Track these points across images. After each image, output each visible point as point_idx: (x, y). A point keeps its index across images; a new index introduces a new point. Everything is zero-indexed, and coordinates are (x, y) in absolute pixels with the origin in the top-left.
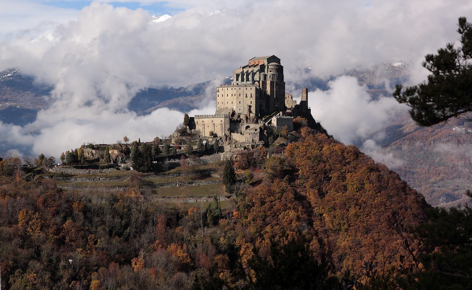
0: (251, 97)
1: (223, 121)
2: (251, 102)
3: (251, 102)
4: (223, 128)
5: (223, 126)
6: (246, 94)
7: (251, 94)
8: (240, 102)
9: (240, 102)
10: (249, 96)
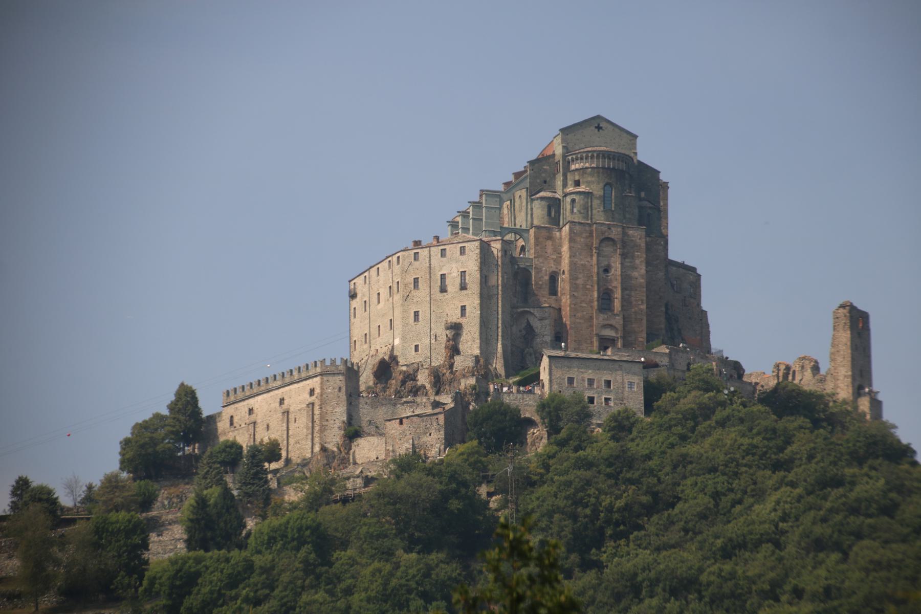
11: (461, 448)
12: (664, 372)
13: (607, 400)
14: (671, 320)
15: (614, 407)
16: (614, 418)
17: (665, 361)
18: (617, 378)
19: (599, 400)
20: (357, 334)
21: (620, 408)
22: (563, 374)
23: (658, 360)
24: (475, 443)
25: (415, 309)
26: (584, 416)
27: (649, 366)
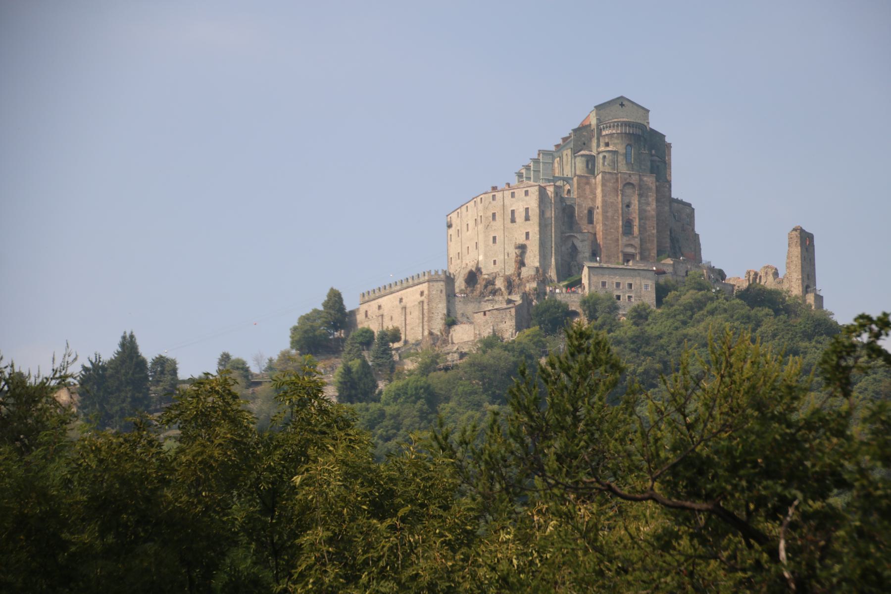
0: (527, 219)
1: (426, 292)
2: (527, 234)
3: (527, 234)
4: (426, 311)
5: (426, 307)
6: (513, 212)
7: (527, 209)
8: (494, 238)
9: (494, 238)
11: (527, 332)
12: (669, 277)
13: (630, 297)
14: (674, 240)
15: (635, 302)
16: (635, 310)
17: (670, 270)
18: (636, 281)
19: (624, 298)
20: (453, 253)
22: (598, 280)
23: (665, 269)
24: (537, 328)
25: (496, 236)
27: (660, 273)
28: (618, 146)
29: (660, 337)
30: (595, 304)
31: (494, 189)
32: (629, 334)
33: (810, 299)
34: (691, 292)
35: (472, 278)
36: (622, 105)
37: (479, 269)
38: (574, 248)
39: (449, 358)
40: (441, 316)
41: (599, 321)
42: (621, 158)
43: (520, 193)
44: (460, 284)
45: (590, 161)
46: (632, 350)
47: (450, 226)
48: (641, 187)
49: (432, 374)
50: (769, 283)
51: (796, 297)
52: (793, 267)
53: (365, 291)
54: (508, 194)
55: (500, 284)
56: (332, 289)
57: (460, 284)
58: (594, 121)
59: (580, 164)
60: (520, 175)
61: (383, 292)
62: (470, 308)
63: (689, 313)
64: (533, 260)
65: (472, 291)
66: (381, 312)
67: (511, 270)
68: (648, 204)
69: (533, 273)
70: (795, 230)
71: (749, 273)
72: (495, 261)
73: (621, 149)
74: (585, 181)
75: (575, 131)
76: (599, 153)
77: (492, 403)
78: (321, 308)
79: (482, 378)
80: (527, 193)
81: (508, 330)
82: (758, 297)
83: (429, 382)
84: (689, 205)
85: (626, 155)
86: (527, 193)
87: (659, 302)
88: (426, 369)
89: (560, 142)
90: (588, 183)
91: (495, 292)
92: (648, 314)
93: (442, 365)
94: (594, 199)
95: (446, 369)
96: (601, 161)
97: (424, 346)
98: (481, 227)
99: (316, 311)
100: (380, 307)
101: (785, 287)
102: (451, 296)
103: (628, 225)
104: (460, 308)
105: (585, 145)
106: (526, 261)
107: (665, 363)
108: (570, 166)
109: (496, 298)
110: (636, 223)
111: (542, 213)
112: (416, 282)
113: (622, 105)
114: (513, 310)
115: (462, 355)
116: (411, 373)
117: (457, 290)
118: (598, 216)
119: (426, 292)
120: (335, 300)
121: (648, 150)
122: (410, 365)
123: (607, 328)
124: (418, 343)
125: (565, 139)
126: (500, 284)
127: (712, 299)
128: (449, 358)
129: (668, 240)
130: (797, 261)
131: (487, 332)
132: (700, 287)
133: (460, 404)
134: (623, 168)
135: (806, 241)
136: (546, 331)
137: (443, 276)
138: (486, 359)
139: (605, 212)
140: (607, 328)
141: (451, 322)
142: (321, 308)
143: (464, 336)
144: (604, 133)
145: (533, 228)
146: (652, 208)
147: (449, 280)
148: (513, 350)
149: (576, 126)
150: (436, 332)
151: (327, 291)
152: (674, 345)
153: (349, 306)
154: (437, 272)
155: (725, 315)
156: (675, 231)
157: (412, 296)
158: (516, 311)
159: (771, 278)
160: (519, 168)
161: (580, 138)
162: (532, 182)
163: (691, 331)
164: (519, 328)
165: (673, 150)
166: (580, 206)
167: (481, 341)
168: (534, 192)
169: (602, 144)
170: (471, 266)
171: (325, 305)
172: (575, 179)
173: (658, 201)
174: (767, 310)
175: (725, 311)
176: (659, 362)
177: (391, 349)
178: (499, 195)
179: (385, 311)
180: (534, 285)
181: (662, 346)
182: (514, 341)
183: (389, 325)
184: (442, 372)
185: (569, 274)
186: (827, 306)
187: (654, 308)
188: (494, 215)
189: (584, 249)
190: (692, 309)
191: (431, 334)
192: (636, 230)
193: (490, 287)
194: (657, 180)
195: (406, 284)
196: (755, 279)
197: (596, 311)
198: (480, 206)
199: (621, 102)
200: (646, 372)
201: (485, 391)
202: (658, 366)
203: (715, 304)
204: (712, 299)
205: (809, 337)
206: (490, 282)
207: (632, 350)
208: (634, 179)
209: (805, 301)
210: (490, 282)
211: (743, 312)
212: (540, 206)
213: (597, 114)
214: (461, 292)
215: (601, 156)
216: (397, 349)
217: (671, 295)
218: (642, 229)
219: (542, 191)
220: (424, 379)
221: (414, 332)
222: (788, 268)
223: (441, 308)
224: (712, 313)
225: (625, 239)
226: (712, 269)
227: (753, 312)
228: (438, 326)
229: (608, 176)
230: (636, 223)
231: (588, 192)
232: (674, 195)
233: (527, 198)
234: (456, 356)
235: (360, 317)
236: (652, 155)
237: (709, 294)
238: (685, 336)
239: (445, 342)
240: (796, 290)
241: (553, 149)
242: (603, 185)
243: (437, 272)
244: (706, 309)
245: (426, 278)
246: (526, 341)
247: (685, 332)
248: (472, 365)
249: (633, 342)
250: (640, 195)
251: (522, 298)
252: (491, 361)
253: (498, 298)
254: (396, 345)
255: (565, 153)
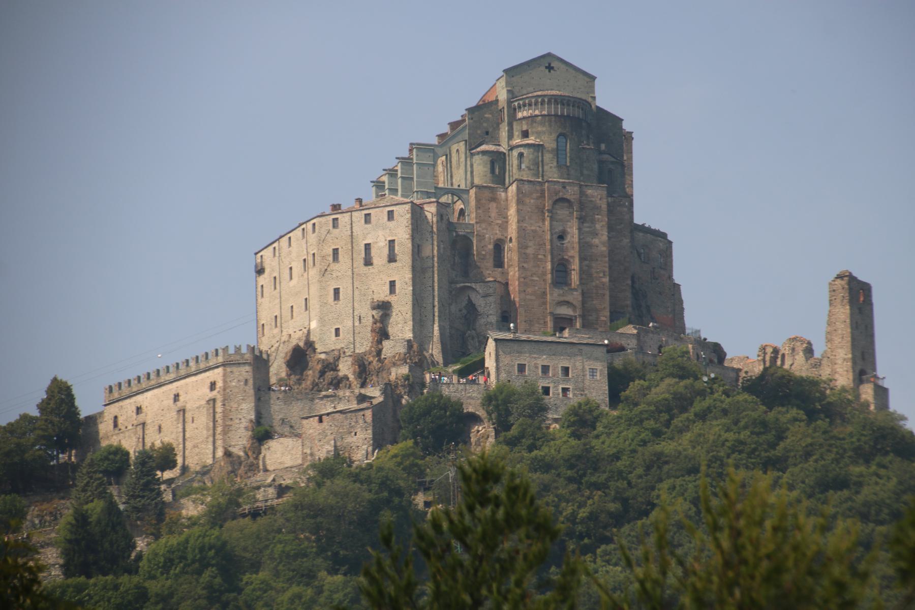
0: (392, 258)
1: (220, 384)
2: (392, 284)
3: (392, 284)
4: (219, 416)
5: (219, 409)
6: (368, 247)
7: (392, 242)
8: (337, 291)
9: (337, 291)
10: (380, 255)
11: (394, 449)
13: (565, 390)
14: (638, 295)
15: (574, 399)
16: (574, 412)
17: (632, 344)
18: (577, 364)
19: (556, 391)
20: (265, 317)
21: (581, 399)
22: (511, 361)
23: (623, 342)
24: (410, 443)
26: (539, 409)
27: (613, 349)
28: (544, 136)
29: (617, 457)
30: (506, 401)
31: (336, 208)
32: (565, 451)
33: (867, 393)
34: (668, 381)
35: (299, 358)
36: (550, 68)
37: (310, 344)
38: (471, 307)
39: (260, 495)
40: (245, 423)
41: (514, 431)
42: (548, 157)
43: (380, 215)
44: (278, 369)
45: (497, 161)
46: (570, 480)
47: (260, 271)
48: (582, 206)
49: (229, 524)
50: (797, 365)
51: (844, 389)
52: (837, 340)
53: (113, 382)
54: (359, 216)
55: (346, 368)
56: (55, 380)
57: (278, 369)
58: (502, 95)
59: (480, 167)
60: (379, 185)
61: (144, 384)
62: (296, 410)
63: (665, 417)
64: (402, 328)
65: (299, 382)
66: (141, 417)
67: (364, 345)
68: (595, 234)
69: (402, 349)
70: (840, 277)
71: (763, 349)
72: (338, 330)
73: (549, 141)
74: (488, 194)
75: (470, 110)
76: (512, 149)
77: (333, 571)
78: (35, 413)
79: (316, 530)
80: (391, 215)
81: (360, 446)
82: (779, 388)
83: (225, 536)
84: (664, 236)
85: (557, 152)
86: (391, 215)
87: (615, 398)
88: (219, 515)
89: (446, 129)
90: (494, 199)
91: (337, 383)
92: (597, 419)
93: (246, 508)
94: (504, 226)
95: (255, 514)
96: (516, 162)
97: (216, 475)
98: (313, 272)
99: (25, 418)
100: (139, 410)
101: (825, 373)
102: (262, 389)
103: (561, 270)
104: (277, 409)
105: (489, 135)
106: (391, 330)
107: (625, 501)
108: (463, 171)
109: (340, 393)
110: (575, 265)
111: (417, 250)
112: (202, 366)
113: (550, 68)
114: (369, 413)
115: (282, 491)
116: (193, 522)
117: (273, 380)
118: (511, 254)
119: (220, 384)
120: (60, 397)
121: (594, 143)
122: (191, 509)
123: (526, 442)
124: (205, 471)
125: (454, 125)
126: (346, 368)
127: (702, 393)
128: (260, 495)
129: (629, 294)
130: (844, 329)
131: (324, 451)
132: (683, 373)
133: (277, 574)
134: (552, 173)
135: (858, 295)
136: (425, 449)
137: (248, 356)
138: (323, 497)
139: (522, 247)
140: (526, 442)
141: (262, 434)
142: (35, 413)
143: (283, 456)
144: (520, 115)
145: (403, 274)
146: (601, 241)
147: (260, 362)
148: (369, 481)
149: (474, 104)
150: (237, 451)
151: (47, 383)
152: (640, 471)
153: (85, 407)
154: (238, 349)
155: (724, 421)
156: (641, 277)
157: (196, 391)
158: (374, 415)
159: (800, 357)
160: (377, 173)
161: (480, 123)
162: (399, 198)
163: (667, 447)
164: (378, 442)
165: (635, 143)
166: (481, 237)
167: (313, 466)
168: (403, 213)
169: (516, 133)
170: (298, 339)
171: (42, 407)
172: (473, 192)
173: (610, 228)
174: (794, 412)
175: (725, 412)
176: (614, 500)
177: (159, 482)
178: (344, 219)
179: (149, 416)
180: (404, 370)
181: (620, 473)
182: (370, 466)
183: (155, 440)
184: (247, 520)
185: (463, 352)
186: (896, 405)
187: (605, 408)
188: (336, 252)
189: (489, 309)
190: (669, 410)
191: (228, 454)
192: (575, 277)
193: (329, 375)
194: (610, 195)
195: (185, 370)
196: (774, 360)
197: (508, 413)
198: (312, 238)
199: (548, 62)
200: (593, 517)
201: (322, 550)
202: (613, 507)
203: (708, 402)
204: (702, 393)
205: (864, 456)
206: (330, 366)
207: (570, 480)
208: (571, 193)
209: (858, 396)
210: (330, 366)
211: (754, 415)
212: (413, 238)
213: (508, 83)
214: (281, 382)
215: (515, 153)
216: (170, 482)
217: (635, 386)
218: (585, 274)
219: (417, 212)
220: (216, 532)
221: (199, 451)
222: (829, 340)
223: (246, 410)
224: (702, 416)
225: (557, 292)
226: (702, 343)
227: (771, 415)
228: (240, 440)
229: (526, 187)
230: (575, 265)
231: (493, 214)
232: (638, 220)
233: (391, 224)
234: (271, 491)
235: (105, 427)
236: (601, 153)
237: (698, 385)
238: (659, 455)
239: (253, 468)
240: (843, 378)
241: (435, 141)
242: (520, 202)
243: (238, 349)
244: (693, 410)
245: (220, 359)
246: (391, 464)
247: (658, 448)
248: (296, 507)
249: (571, 467)
250: (582, 220)
251: (384, 392)
252: (332, 500)
253: (343, 393)
254: (168, 475)
255: (454, 148)
